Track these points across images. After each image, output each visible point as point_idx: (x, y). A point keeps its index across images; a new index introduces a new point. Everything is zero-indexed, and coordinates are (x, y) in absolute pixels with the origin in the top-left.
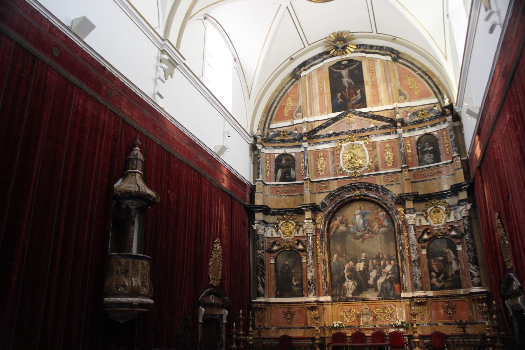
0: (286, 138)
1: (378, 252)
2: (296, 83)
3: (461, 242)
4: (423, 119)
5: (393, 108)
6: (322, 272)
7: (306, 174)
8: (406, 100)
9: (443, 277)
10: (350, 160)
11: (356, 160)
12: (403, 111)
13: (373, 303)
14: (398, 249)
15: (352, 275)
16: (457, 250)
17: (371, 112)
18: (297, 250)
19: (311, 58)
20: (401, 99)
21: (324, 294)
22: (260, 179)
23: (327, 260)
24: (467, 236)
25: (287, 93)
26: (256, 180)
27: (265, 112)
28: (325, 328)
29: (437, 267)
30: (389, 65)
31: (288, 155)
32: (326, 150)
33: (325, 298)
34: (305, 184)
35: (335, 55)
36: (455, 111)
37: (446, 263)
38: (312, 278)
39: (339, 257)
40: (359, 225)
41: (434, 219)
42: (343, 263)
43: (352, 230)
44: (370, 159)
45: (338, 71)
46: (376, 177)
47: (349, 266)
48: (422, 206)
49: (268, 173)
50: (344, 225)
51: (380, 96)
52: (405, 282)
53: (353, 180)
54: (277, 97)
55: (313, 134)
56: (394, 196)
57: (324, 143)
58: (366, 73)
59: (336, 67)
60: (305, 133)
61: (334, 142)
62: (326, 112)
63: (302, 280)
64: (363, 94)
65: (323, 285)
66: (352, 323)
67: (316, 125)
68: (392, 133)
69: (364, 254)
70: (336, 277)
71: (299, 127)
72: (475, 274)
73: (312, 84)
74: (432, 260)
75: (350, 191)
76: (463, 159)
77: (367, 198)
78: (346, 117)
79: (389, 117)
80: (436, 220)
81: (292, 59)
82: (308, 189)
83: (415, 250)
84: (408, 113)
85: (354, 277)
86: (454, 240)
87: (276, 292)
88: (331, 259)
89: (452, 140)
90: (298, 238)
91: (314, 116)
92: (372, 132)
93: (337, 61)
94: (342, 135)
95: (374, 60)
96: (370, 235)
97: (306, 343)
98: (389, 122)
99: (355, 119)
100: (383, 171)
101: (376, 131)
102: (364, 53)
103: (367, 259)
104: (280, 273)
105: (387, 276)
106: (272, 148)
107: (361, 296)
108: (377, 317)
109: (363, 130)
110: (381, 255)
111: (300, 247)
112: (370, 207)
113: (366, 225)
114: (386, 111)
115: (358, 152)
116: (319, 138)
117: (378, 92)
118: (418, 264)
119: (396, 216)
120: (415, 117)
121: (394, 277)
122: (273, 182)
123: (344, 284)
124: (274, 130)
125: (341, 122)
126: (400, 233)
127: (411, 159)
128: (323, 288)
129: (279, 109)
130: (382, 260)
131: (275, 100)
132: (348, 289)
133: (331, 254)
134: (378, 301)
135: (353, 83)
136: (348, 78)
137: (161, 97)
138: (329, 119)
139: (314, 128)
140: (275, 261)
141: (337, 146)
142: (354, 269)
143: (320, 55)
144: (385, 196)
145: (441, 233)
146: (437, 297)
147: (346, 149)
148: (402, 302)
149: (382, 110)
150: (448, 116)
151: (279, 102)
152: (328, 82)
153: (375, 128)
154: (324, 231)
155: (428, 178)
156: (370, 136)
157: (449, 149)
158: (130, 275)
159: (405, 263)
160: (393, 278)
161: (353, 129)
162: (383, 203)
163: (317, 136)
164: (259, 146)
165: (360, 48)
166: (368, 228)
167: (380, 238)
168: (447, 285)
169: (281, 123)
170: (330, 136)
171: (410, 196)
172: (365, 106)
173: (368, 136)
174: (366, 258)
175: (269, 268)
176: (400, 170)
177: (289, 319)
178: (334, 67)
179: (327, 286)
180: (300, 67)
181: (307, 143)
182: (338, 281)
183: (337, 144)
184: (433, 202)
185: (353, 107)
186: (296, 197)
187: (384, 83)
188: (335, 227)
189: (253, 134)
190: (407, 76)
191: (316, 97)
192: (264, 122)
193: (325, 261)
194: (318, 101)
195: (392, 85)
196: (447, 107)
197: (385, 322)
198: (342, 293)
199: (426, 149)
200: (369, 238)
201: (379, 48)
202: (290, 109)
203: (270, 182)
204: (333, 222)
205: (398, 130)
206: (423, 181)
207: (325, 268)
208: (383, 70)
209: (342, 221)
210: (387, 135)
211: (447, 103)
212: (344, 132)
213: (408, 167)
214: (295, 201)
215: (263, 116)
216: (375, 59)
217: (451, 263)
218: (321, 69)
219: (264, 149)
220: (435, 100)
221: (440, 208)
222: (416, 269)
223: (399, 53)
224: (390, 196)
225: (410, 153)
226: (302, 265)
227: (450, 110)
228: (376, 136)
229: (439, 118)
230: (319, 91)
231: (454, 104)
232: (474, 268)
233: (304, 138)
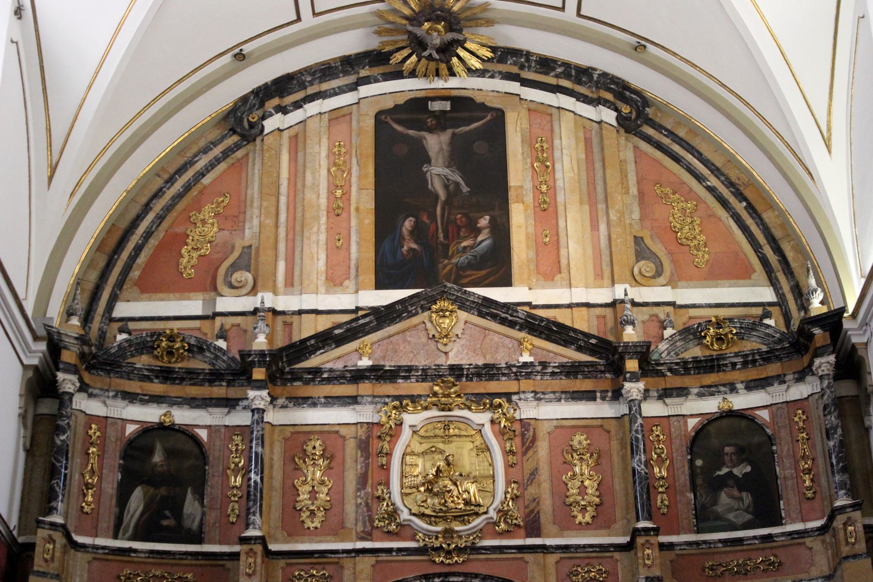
0: (180, 365)
2: (239, 154)
4: (721, 357)
5: (609, 300)
7: (252, 518)
8: (662, 280)
10: (430, 482)
11: (455, 484)
12: (646, 317)
17: (529, 304)
19: (310, 67)
22: (58, 519)
25: (199, 187)
26: (39, 522)
27: (98, 250)
30: (606, 142)
31: (180, 435)
32: (337, 432)
34: (243, 557)
35: (405, 75)
36: (847, 338)
44: (508, 483)
45: (411, 132)
46: (529, 557)
49: (90, 499)
51: (563, 252)
54: (158, 194)
55: (290, 362)
57: (332, 401)
58: (520, 157)
59: (403, 116)
60: (262, 354)
61: (372, 403)
62: (350, 284)
67: (308, 328)
68: (598, 395)
71: (238, 325)
73: (304, 166)
78: (426, 314)
79: (594, 332)
81: (240, 57)
84: (665, 328)
89: (831, 443)
91: (301, 294)
92: (525, 384)
93: (412, 95)
94: (406, 378)
95: (551, 115)
99: (461, 325)
100: (555, 536)
101: (538, 382)
102: (517, 84)
106: (115, 397)
109: (489, 372)
114: (584, 310)
115: (465, 452)
116: (313, 380)
117: (558, 235)
120: (691, 344)
122: (106, 537)
124: (132, 325)
125: (408, 329)
127: (666, 503)
129: (162, 246)
131: (147, 208)
135: (465, 189)
136: (448, 167)
138: (361, 313)
139: (296, 338)
141: (384, 419)
143: (349, 63)
147: (415, 436)
149: (566, 301)
151: (161, 218)
152: (371, 170)
153: (539, 368)
156: (515, 398)
157: (812, 480)
161: (449, 363)
163: (309, 371)
164: (67, 381)
165: (501, 60)
169: (162, 300)
170: (358, 376)
172: (506, 281)
173: (508, 396)
176: (624, 540)
178: (399, 116)
181: (264, 393)
183: (382, 414)
185: (461, 276)
187: (581, 203)
189: (48, 327)
190: (668, 190)
191: (317, 218)
192: (90, 286)
194: (323, 237)
195: (613, 216)
196: (819, 320)
199: (724, 471)
201: (573, 72)
202: (206, 250)
203: (96, 536)
205: (627, 385)
208: (583, 156)
210: (580, 399)
211: (816, 306)
212: (417, 370)
215: (88, 264)
216: (555, 111)
218: (344, 116)
219: (83, 395)
220: (767, 295)
225: (663, 478)
227: (828, 334)
228: (540, 399)
229: (779, 359)
230: (328, 199)
231: (845, 315)
233: (254, 370)
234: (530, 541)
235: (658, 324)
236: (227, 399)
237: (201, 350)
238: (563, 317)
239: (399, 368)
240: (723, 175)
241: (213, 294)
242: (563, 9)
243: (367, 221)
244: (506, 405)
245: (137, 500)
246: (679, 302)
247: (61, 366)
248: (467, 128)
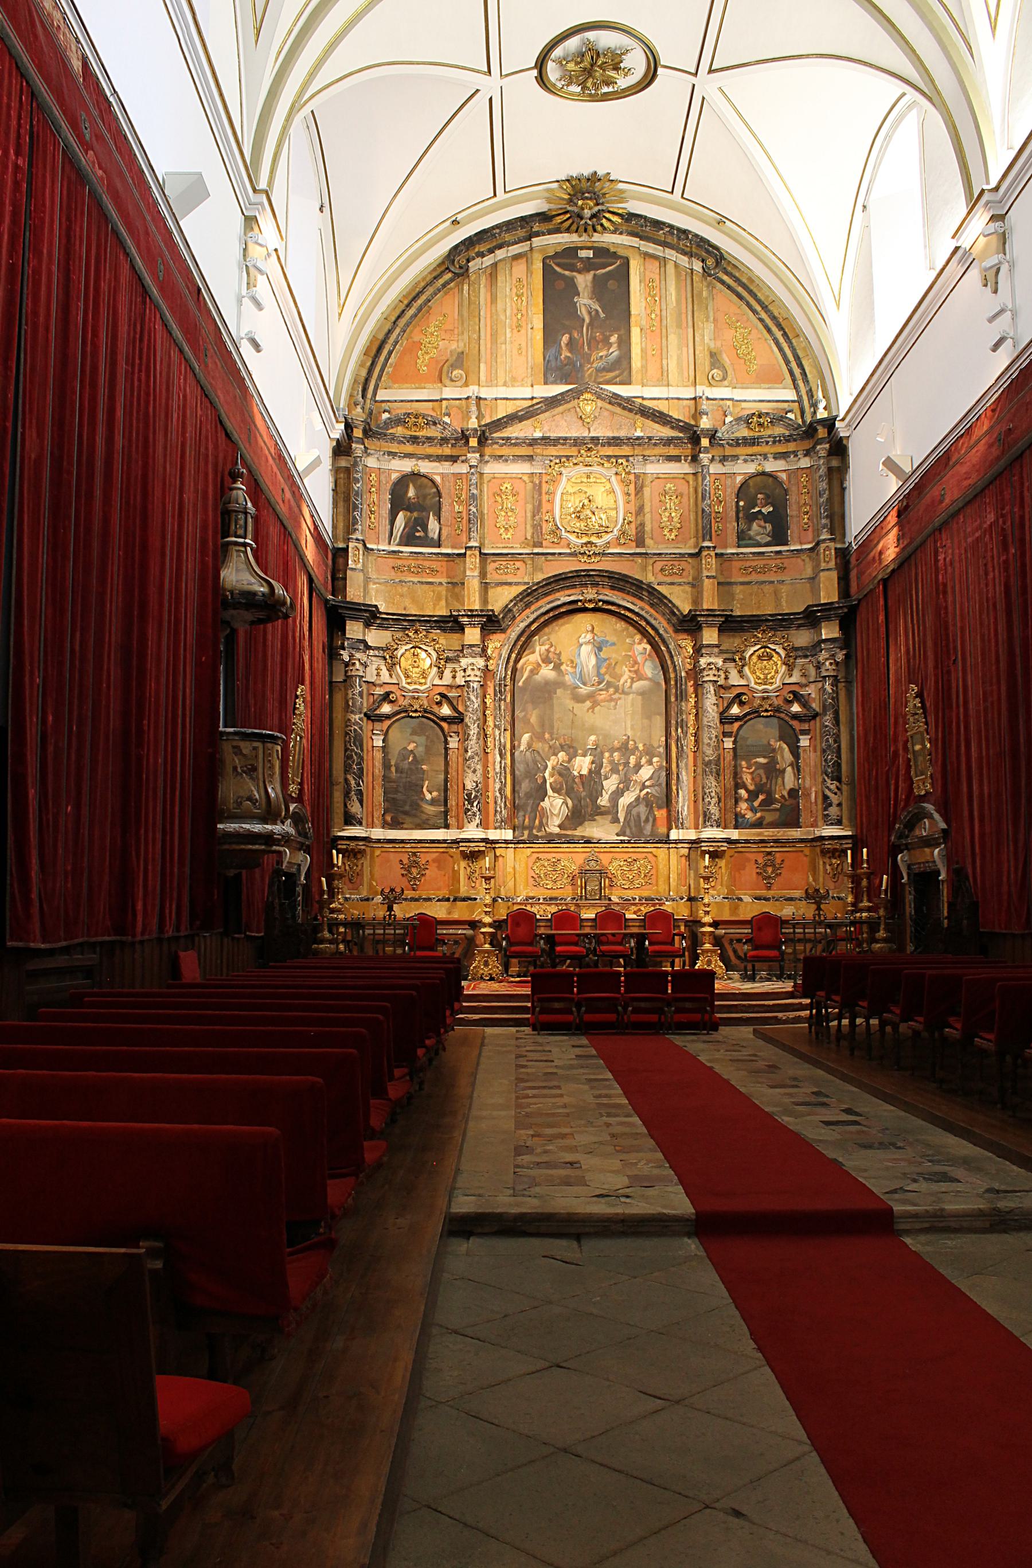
1: (625, 735)
3: (809, 730)
5: (693, 396)
6: (497, 773)
8: (726, 383)
9: (762, 800)
10: (578, 512)
11: (594, 514)
13: (608, 850)
14: (673, 733)
16: (798, 747)
17: (643, 399)
18: (437, 717)
20: (713, 377)
21: (498, 824)
22: (360, 538)
23: (508, 746)
24: (828, 717)
26: (349, 539)
28: (497, 901)
29: (753, 779)
31: (423, 478)
34: (468, 559)
37: (773, 771)
38: (477, 786)
41: (758, 674)
43: (568, 679)
45: (567, 273)
48: (734, 642)
52: (683, 805)
53: (583, 560)
57: (518, 458)
60: (475, 430)
63: (446, 790)
64: (625, 343)
65: (496, 803)
66: (561, 891)
67: (503, 411)
69: (593, 738)
70: (525, 786)
72: (834, 799)
74: (744, 763)
75: (574, 587)
76: (839, 546)
77: (613, 608)
78: (576, 400)
79: (681, 418)
80: (762, 676)
82: (476, 573)
83: (714, 739)
86: (795, 724)
87: (383, 815)
88: (516, 743)
89: (822, 500)
90: (443, 690)
92: (638, 451)
94: (563, 444)
96: (611, 695)
97: (460, 932)
98: (681, 429)
103: (599, 749)
104: (393, 769)
105: (641, 791)
107: (579, 832)
108: (614, 879)
109: (615, 441)
110: (631, 743)
111: (446, 710)
113: (603, 670)
114: (676, 401)
116: (505, 444)
118: (717, 771)
126: (682, 696)
128: (496, 811)
134: (621, 845)
135: (602, 315)
136: (591, 299)
137: (257, 347)
138: (535, 401)
140: (384, 741)
142: (569, 769)
145: (770, 705)
146: (747, 841)
148: (671, 850)
149: (666, 396)
150: (819, 442)
154: (505, 677)
155: (754, 577)
156: (631, 459)
157: (808, 519)
158: (261, 776)
159: (686, 765)
160: (653, 795)
161: (590, 435)
163: (503, 439)
164: (357, 448)
166: (607, 677)
167: (633, 705)
168: (769, 817)
170: (533, 442)
171: (715, 616)
172: (627, 382)
173: (627, 457)
175: (370, 757)
177: (415, 878)
180: (469, 243)
181: (478, 455)
182: (528, 795)
184: (760, 635)
186: (440, 588)
188: (529, 668)
196: (822, 421)
197: (630, 891)
198: (537, 822)
199: (757, 509)
201: (675, 232)
204: (527, 655)
205: (701, 455)
206: (742, 583)
209: (547, 656)
211: (822, 414)
213: (714, 547)
214: (439, 598)
215: (362, 365)
217: (784, 771)
219: (365, 455)
220: (790, 395)
221: (774, 650)
222: (711, 782)
223: (722, 257)
226: (446, 755)
227: (826, 430)
229: (795, 440)
231: (838, 419)
232: (833, 787)
234: (638, 550)
235: (722, 413)
236: (452, 456)
237: (435, 424)
238: (662, 407)
239: (560, 438)
240: (769, 311)
241: (439, 385)
242: (672, 192)
243: (538, 337)
244: (625, 463)
245: (401, 519)
246: (736, 398)
247: (354, 439)
248: (603, 271)
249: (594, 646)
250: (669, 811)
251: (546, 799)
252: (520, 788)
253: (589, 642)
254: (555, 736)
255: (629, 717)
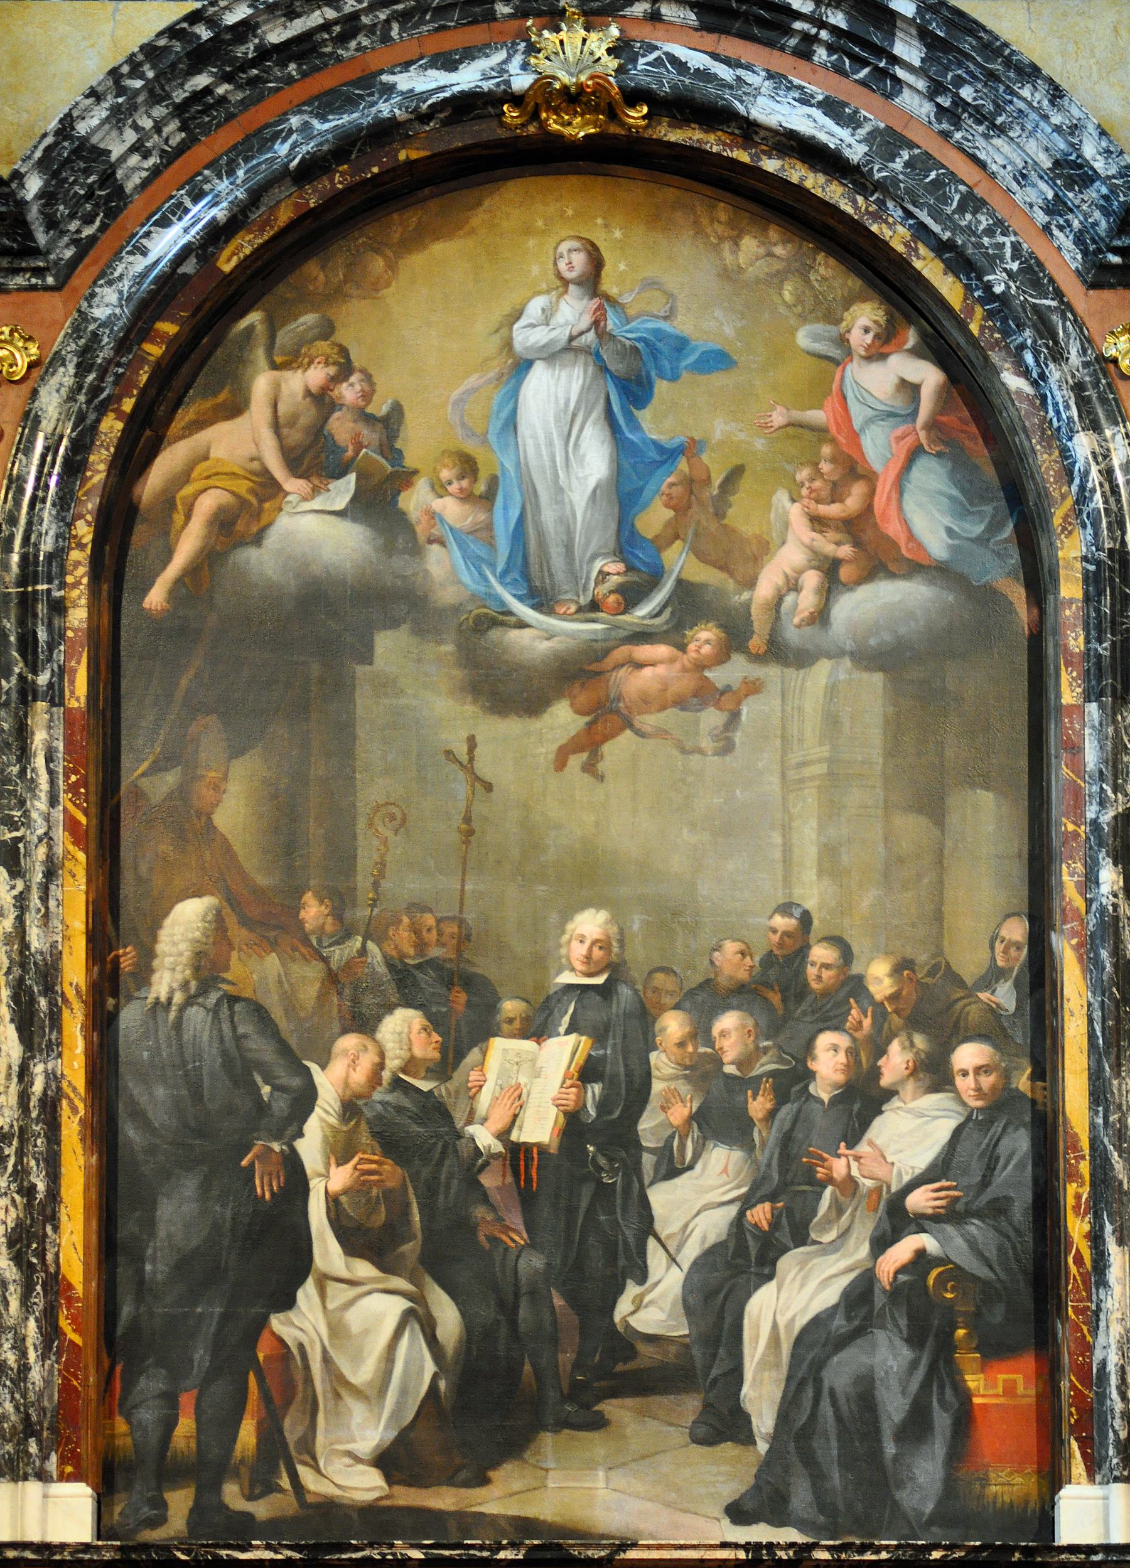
1: (785, 909)
15: (396, 1201)
33: (18, 1512)
39: (238, 933)
40: (548, 516)
42: (293, 1042)
47: (375, 1079)
50: (342, 491)
56: (1090, 150)
77: (712, 142)
85: (427, 1229)
88: (127, 957)
96: (700, 666)
103: (625, 991)
105: (881, 1244)
110: (821, 953)
112: (729, 276)
119: (1082, 445)
121: (982, 1271)
123: (277, 1323)
130: (837, 1028)
132: (339, 1382)
133: (128, 888)
144: (972, 134)
154: (58, 556)
160: (956, 1274)
162: (921, 231)
167: (831, 723)
174: (616, 970)
179: (51, 1332)
188: (207, 504)
193: (49, 989)
198: (247, 1435)
200: (680, 703)
204: (200, 424)
207: (38, 1087)
209: (318, 433)
224: (1032, 146)
249: (603, 369)
250: (1050, 1372)
251: (307, 1294)
252: (150, 1224)
253: (570, 348)
254: (363, 913)
255: (808, 803)
